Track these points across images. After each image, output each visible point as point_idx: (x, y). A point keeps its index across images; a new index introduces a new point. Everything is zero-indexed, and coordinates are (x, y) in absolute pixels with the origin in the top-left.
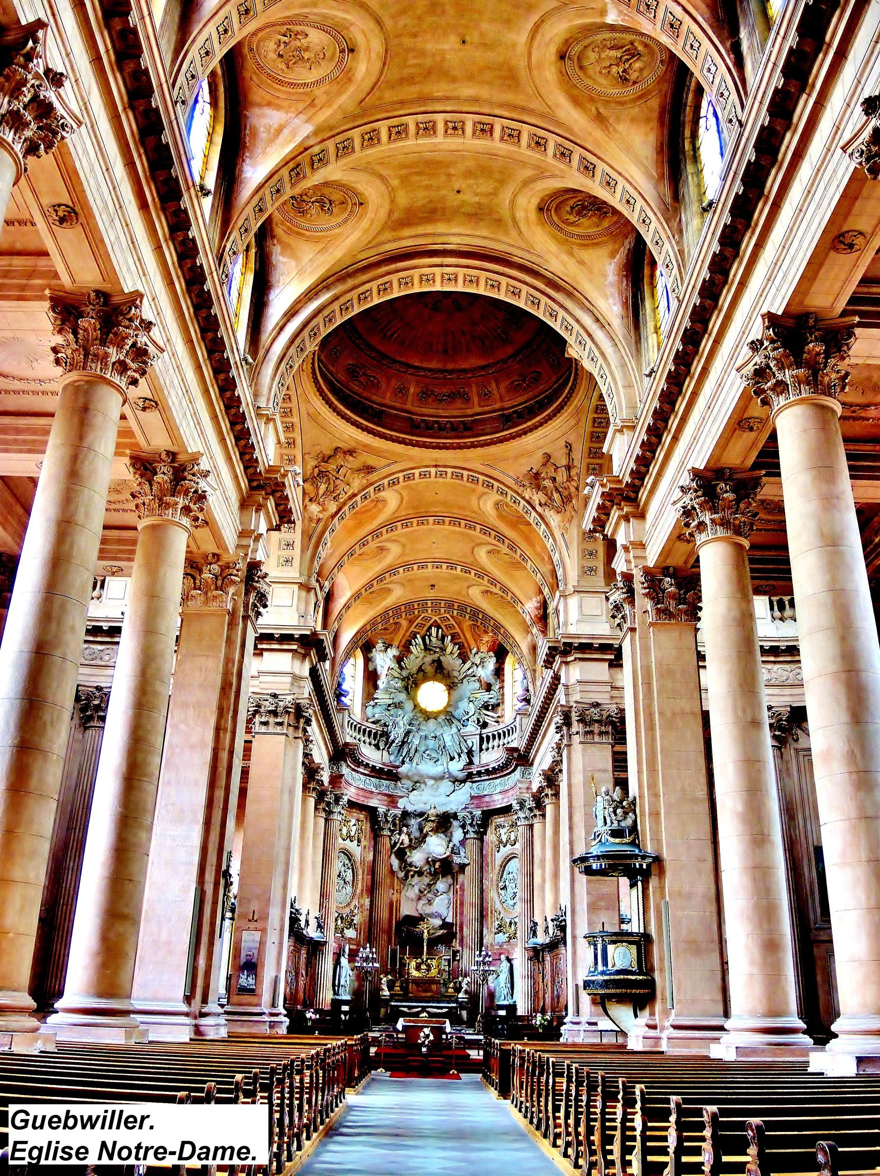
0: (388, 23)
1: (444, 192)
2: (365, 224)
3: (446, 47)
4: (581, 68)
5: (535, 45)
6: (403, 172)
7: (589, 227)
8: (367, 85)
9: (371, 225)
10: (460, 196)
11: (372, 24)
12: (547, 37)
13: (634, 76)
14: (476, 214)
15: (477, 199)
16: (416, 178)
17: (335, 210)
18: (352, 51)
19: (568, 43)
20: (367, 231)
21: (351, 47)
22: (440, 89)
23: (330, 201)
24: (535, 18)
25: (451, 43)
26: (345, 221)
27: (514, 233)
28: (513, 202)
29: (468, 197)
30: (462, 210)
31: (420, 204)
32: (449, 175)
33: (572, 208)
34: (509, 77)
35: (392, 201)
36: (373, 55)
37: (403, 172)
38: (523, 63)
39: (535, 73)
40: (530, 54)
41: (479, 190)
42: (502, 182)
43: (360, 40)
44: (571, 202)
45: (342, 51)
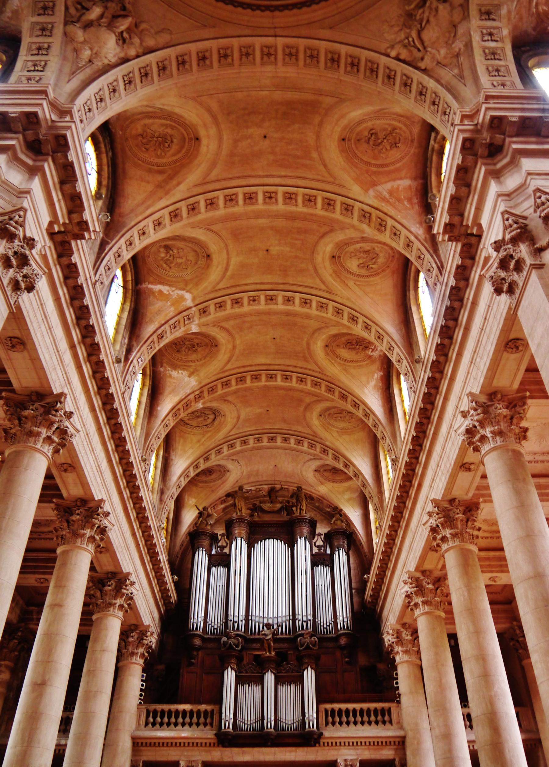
0: (311, 268)
1: (276, 135)
2: (344, 122)
3: (277, 248)
4: (196, 251)
5: (225, 262)
6: (308, 162)
7: (153, 124)
8: (327, 239)
9: (338, 120)
10: (263, 132)
11: (320, 271)
12: (220, 268)
13: (162, 250)
14: (249, 114)
15: (251, 131)
16: (299, 153)
17: (366, 133)
18: (333, 257)
19: (208, 266)
20: (343, 116)
21: (334, 259)
22: (281, 223)
23: (368, 143)
24: (229, 273)
25: (275, 250)
26: (359, 123)
27: (215, 106)
28: (220, 139)
29: (256, 132)
30: (261, 117)
31: (296, 126)
32: (273, 153)
33: (172, 142)
34: (237, 235)
35: (318, 136)
36: (321, 254)
37: (308, 162)
38: (231, 247)
39: (222, 245)
40: (228, 253)
41: (249, 141)
42: (232, 154)
43: (327, 264)
44: (174, 147)
45: (339, 257)
